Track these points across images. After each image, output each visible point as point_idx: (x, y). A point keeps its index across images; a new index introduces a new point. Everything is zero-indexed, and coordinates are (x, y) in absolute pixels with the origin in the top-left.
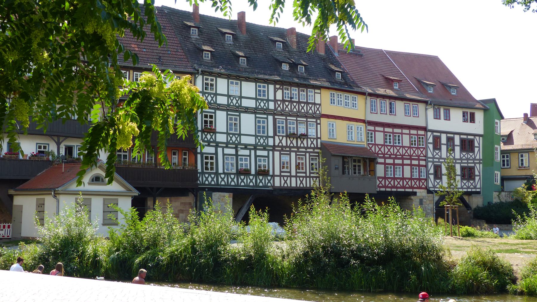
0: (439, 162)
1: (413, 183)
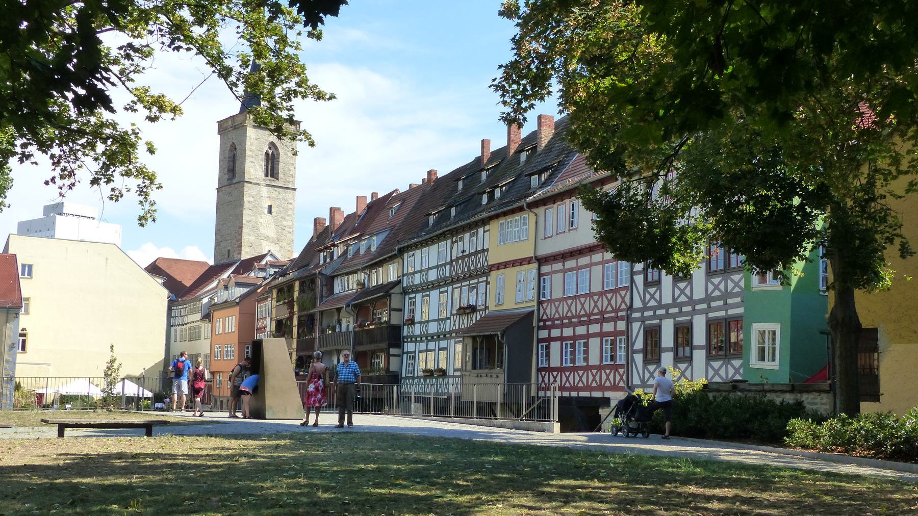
0: (655, 317)
1: (604, 377)
